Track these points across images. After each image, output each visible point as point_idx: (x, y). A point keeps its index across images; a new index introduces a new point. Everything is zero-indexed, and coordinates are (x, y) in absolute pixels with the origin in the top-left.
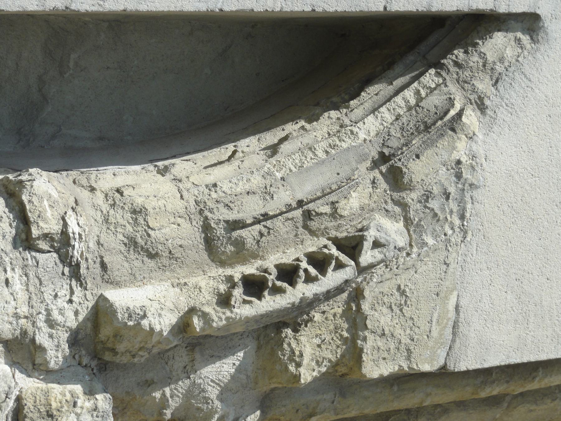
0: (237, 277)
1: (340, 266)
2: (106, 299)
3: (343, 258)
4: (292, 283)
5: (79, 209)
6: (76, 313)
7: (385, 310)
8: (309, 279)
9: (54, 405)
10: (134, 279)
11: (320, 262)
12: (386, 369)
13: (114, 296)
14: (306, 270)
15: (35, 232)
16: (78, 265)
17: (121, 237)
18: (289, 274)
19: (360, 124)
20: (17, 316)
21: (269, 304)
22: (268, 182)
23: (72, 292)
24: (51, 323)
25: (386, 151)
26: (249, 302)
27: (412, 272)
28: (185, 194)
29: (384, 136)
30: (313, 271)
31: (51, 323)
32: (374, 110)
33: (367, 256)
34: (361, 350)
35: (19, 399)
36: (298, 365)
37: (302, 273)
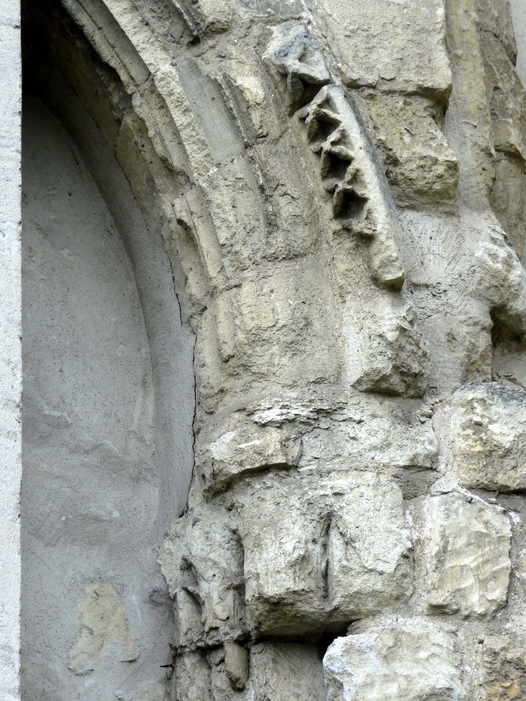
0: (336, 226)
1: (328, 102)
2: (359, 382)
3: (318, 99)
4: (347, 161)
5: (250, 408)
6: (374, 416)
7: (374, 56)
8: (343, 139)
9: (479, 448)
10: (335, 347)
11: (325, 125)
12: (441, 58)
13: (354, 371)
14: (333, 143)
15: (279, 459)
16: (319, 411)
17: (285, 360)
18: (337, 164)
19: (152, 69)
20: (377, 485)
21: (373, 189)
22: (222, 183)
23: (350, 419)
24: (386, 445)
25: (186, 40)
26: (369, 212)
27: (330, 20)
28: (233, 282)
29: (168, 42)
30: (334, 136)
31: (386, 445)
32: (133, 51)
33: (318, 71)
34: (420, 87)
35: (470, 488)
36: (436, 162)
37: (336, 149)
